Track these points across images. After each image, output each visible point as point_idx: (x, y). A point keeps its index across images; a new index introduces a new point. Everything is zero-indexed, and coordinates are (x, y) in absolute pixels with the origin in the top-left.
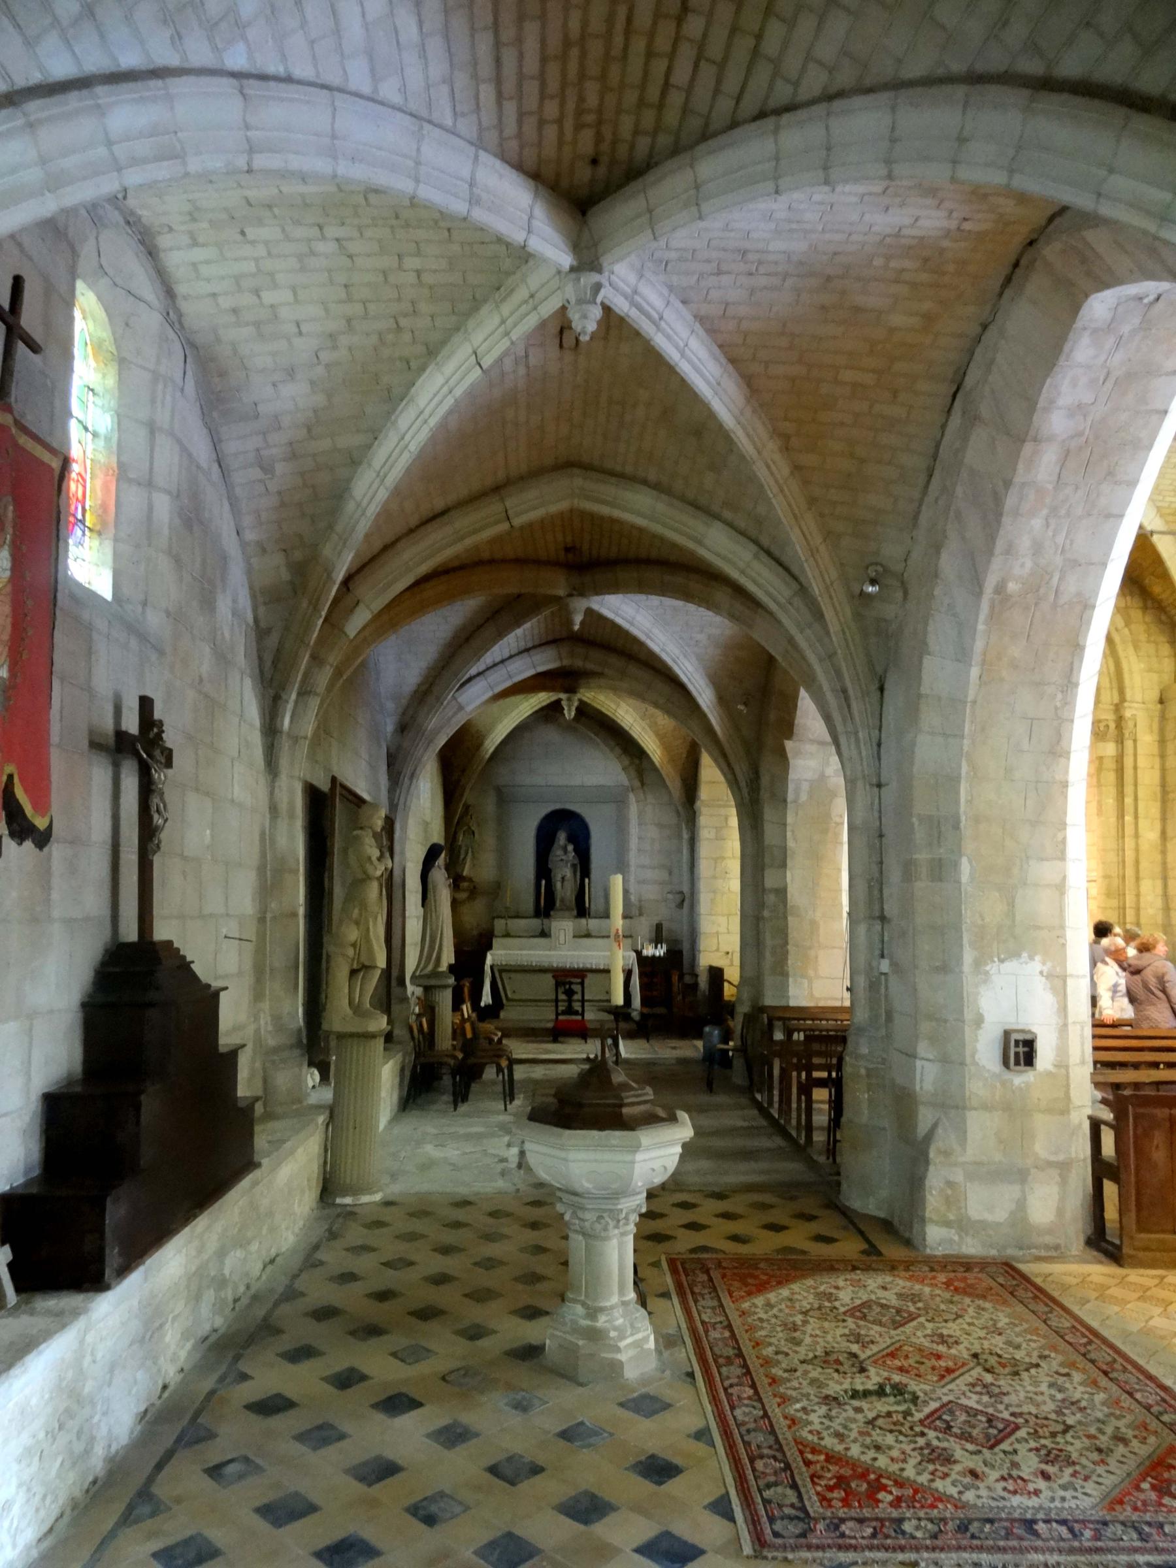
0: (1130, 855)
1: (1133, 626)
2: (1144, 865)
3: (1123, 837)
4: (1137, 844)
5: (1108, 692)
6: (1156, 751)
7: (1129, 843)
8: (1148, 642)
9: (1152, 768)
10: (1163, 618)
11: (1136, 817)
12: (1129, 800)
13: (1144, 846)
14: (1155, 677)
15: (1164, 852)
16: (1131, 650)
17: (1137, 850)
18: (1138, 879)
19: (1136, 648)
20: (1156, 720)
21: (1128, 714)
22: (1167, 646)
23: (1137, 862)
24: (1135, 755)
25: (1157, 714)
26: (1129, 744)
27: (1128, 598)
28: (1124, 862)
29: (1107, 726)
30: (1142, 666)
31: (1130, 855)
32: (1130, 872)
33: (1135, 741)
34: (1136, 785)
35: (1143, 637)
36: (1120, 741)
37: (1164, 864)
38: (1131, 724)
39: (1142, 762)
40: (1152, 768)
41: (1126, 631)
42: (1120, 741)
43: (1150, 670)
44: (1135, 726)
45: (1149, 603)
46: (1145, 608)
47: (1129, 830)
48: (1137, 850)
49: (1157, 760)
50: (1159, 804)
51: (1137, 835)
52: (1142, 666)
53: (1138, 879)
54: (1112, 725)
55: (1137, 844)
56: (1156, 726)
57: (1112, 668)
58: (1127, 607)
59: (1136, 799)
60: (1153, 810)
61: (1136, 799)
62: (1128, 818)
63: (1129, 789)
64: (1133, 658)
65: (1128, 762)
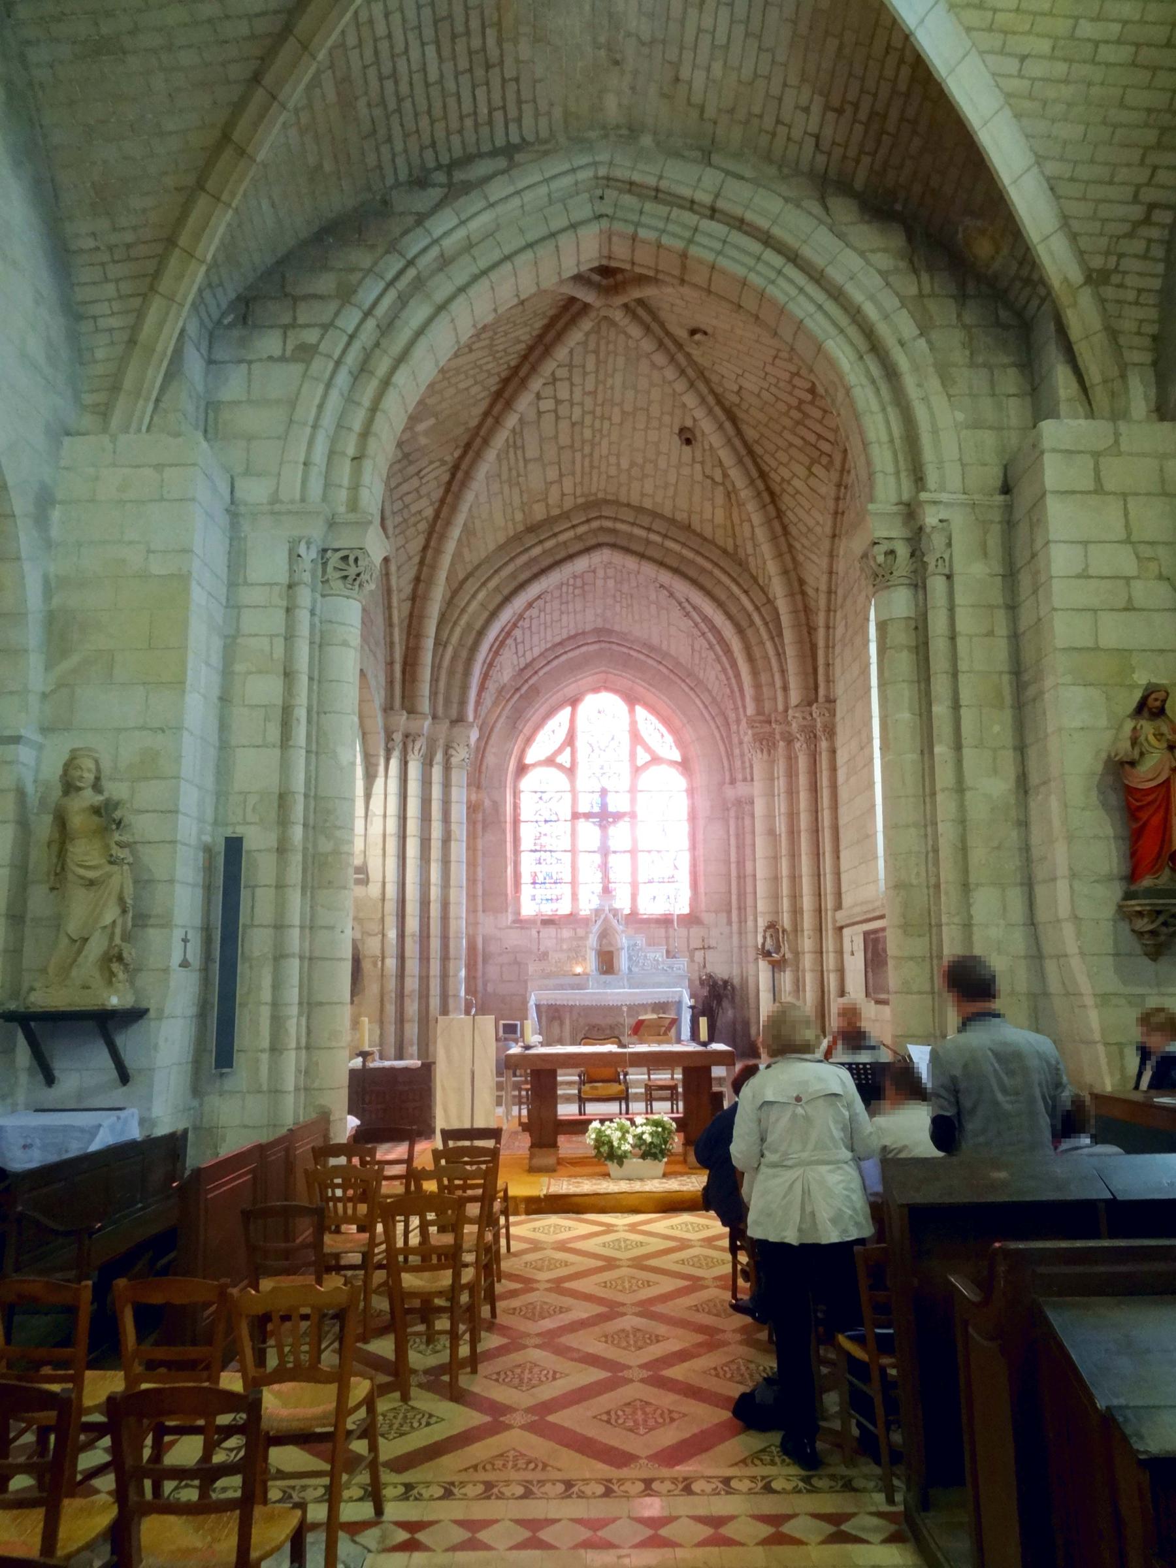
0: (947, 831)
1: (935, 335)
2: (978, 854)
3: (933, 794)
4: (962, 807)
5: (892, 480)
6: (996, 595)
7: (946, 805)
8: (972, 365)
9: (990, 633)
10: (1004, 314)
11: (958, 747)
12: (940, 709)
13: (978, 811)
14: (989, 439)
15: (1024, 824)
16: (934, 383)
17: (962, 821)
18: (966, 887)
19: (946, 379)
20: (996, 529)
21: (931, 518)
22: (1012, 372)
23: (963, 849)
24: (952, 609)
25: (996, 516)
26: (937, 585)
27: (925, 277)
28: (936, 851)
29: (891, 552)
30: (960, 416)
31: (947, 831)
32: (948, 873)
33: (949, 577)
34: (955, 674)
35: (959, 356)
36: (918, 584)
37: (1026, 849)
38: (938, 541)
39: (965, 622)
40: (990, 633)
41: (922, 343)
42: (918, 584)
43: (976, 424)
44: (949, 545)
45: (971, 288)
46: (962, 298)
47: (944, 776)
48: (962, 821)
49: (1001, 616)
50: (1007, 715)
51: (960, 788)
52: (960, 416)
53: (966, 887)
54: (902, 551)
55: (962, 807)
56: (994, 541)
57: (897, 431)
58: (921, 295)
59: (956, 706)
60: (996, 728)
61: (956, 706)
62: (941, 750)
63: (940, 686)
64: (939, 401)
65: (938, 624)
